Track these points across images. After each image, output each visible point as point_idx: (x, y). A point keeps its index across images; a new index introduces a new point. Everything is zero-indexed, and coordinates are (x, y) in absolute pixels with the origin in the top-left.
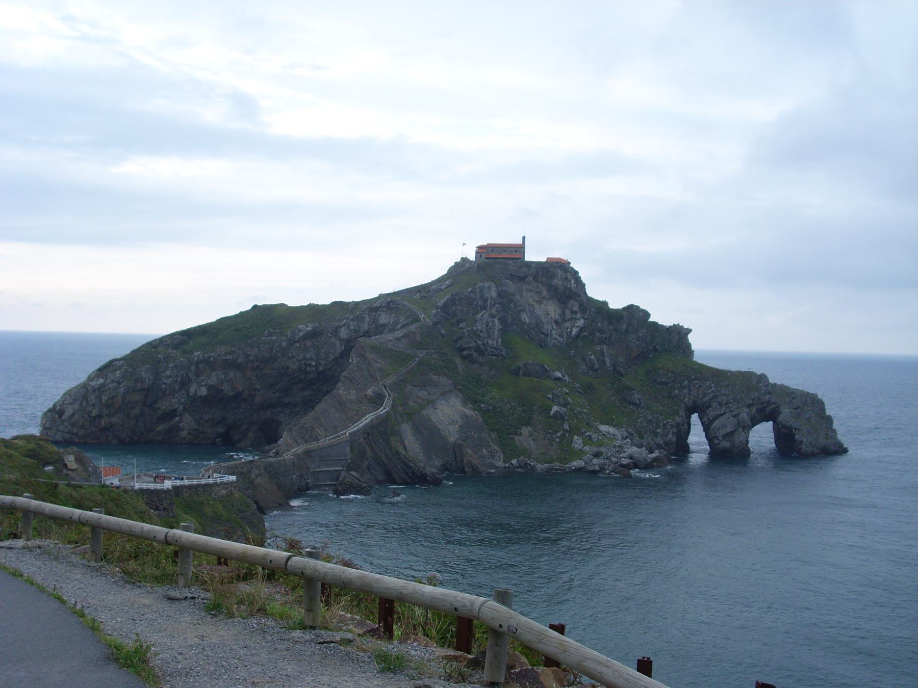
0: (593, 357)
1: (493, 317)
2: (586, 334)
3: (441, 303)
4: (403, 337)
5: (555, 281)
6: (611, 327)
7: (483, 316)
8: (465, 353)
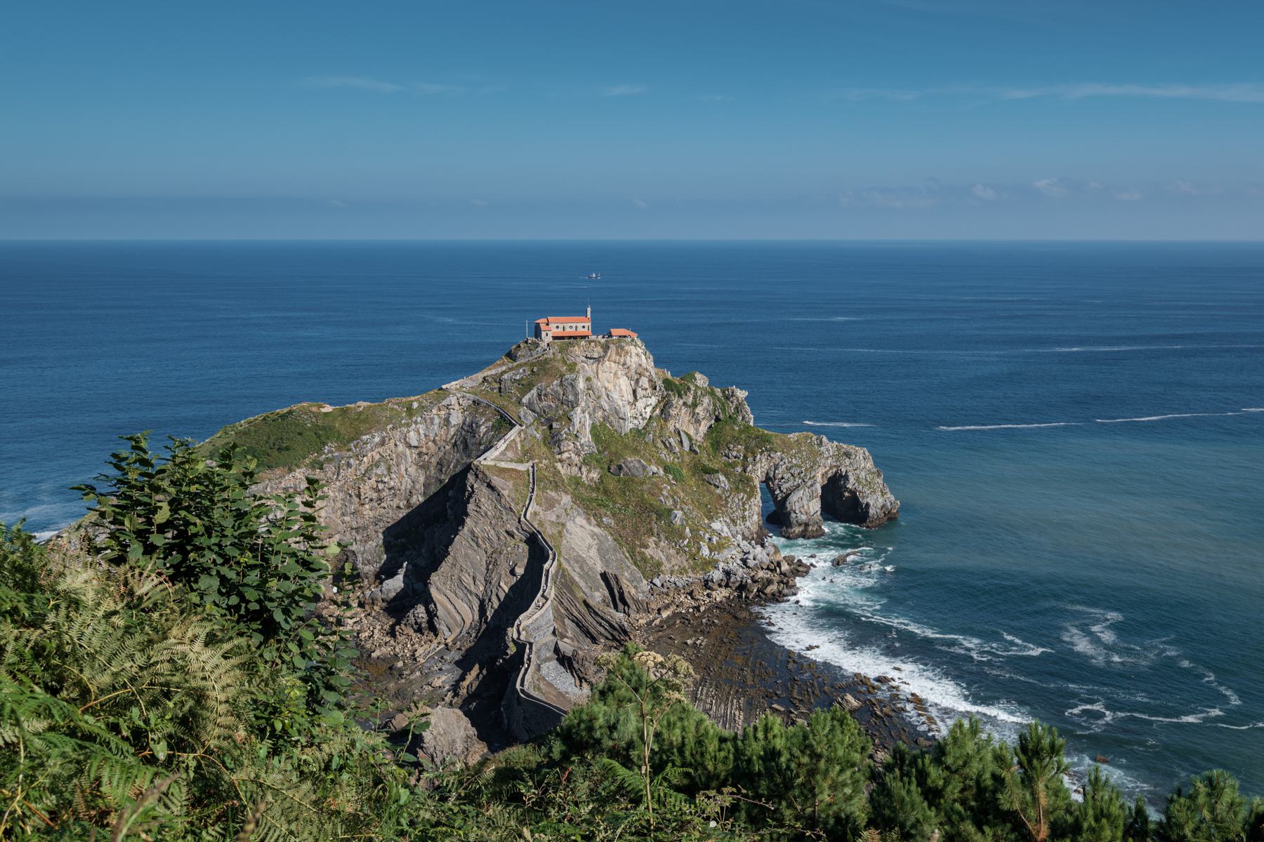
0: (671, 440)
1: (583, 412)
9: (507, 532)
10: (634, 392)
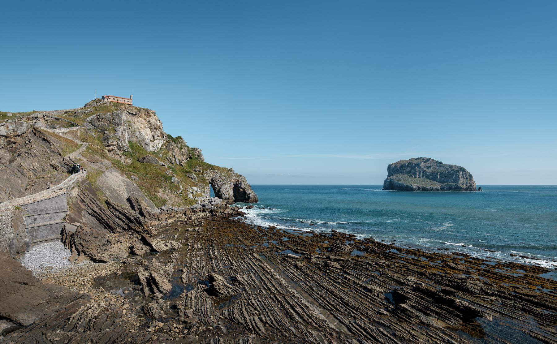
2: (164, 147)
3: (89, 119)
4: (69, 132)
5: (150, 119)
6: (175, 145)
7: (120, 129)
8: (111, 148)
9: (51, 166)
10: (154, 137)
